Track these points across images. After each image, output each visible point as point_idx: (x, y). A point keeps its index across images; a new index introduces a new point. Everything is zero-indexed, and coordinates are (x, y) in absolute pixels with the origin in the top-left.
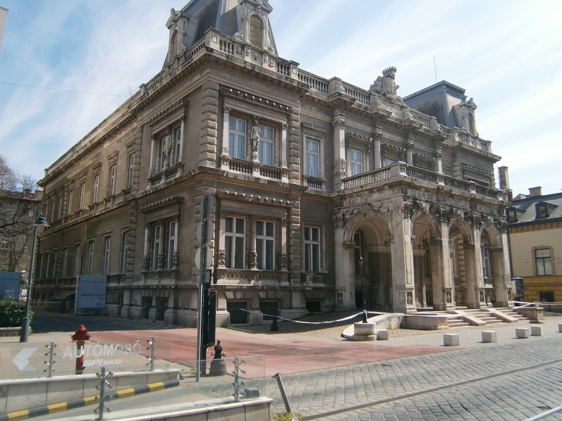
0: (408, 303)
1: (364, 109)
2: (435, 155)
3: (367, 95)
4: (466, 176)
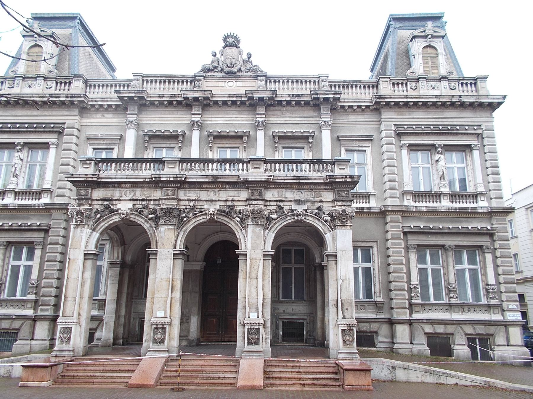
0: (62, 342)
2: (320, 127)
3: (193, 80)
4: (403, 142)
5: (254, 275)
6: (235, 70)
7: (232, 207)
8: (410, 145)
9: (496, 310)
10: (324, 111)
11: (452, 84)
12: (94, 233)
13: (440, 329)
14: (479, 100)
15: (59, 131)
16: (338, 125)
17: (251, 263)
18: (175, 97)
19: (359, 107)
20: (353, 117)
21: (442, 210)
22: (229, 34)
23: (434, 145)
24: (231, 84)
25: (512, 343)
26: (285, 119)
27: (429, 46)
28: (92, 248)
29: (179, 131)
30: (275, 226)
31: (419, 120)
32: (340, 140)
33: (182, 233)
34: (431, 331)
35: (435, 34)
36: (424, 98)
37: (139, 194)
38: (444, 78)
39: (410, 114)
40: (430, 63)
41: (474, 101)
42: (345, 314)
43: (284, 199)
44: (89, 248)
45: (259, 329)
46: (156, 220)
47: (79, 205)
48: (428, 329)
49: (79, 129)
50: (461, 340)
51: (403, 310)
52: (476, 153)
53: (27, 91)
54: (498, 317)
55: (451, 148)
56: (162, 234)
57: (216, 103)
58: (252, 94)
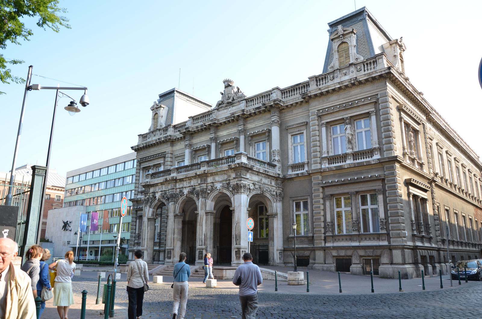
1: (201, 127)
4: (322, 122)
5: (201, 224)
6: (230, 101)
7: (194, 189)
8: (327, 123)
9: (384, 238)
10: (272, 114)
11: (358, 67)
12: (150, 209)
13: (342, 253)
14: (371, 76)
15: (163, 156)
16: (287, 119)
17: (200, 218)
18: (203, 126)
19: (297, 103)
20: (295, 112)
21: (346, 167)
22: (228, 80)
23: (343, 119)
24: (230, 109)
25: (395, 261)
26: (255, 124)
27: (343, 43)
28: (150, 215)
29: (205, 145)
30: (211, 197)
31: (333, 102)
32: (287, 129)
33: (177, 205)
34: (336, 255)
35: (345, 33)
36: (331, 87)
37: (164, 188)
38: (351, 65)
39: (327, 100)
40: (344, 55)
41: (367, 77)
42: (237, 243)
43: (213, 181)
44: (149, 216)
45: (202, 251)
46: (168, 199)
47: (146, 196)
48: (334, 253)
49: (172, 152)
50: (356, 260)
51: (320, 241)
52: (373, 118)
53: (154, 138)
54: (386, 243)
55: (358, 118)
56: (170, 207)
57: (221, 124)
58: (233, 114)
